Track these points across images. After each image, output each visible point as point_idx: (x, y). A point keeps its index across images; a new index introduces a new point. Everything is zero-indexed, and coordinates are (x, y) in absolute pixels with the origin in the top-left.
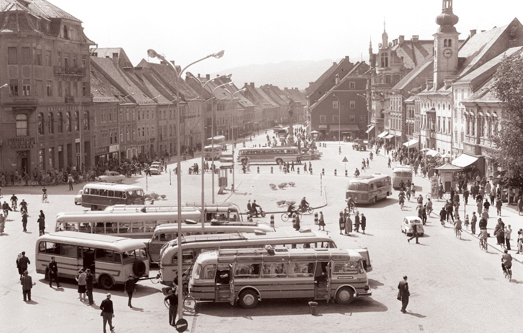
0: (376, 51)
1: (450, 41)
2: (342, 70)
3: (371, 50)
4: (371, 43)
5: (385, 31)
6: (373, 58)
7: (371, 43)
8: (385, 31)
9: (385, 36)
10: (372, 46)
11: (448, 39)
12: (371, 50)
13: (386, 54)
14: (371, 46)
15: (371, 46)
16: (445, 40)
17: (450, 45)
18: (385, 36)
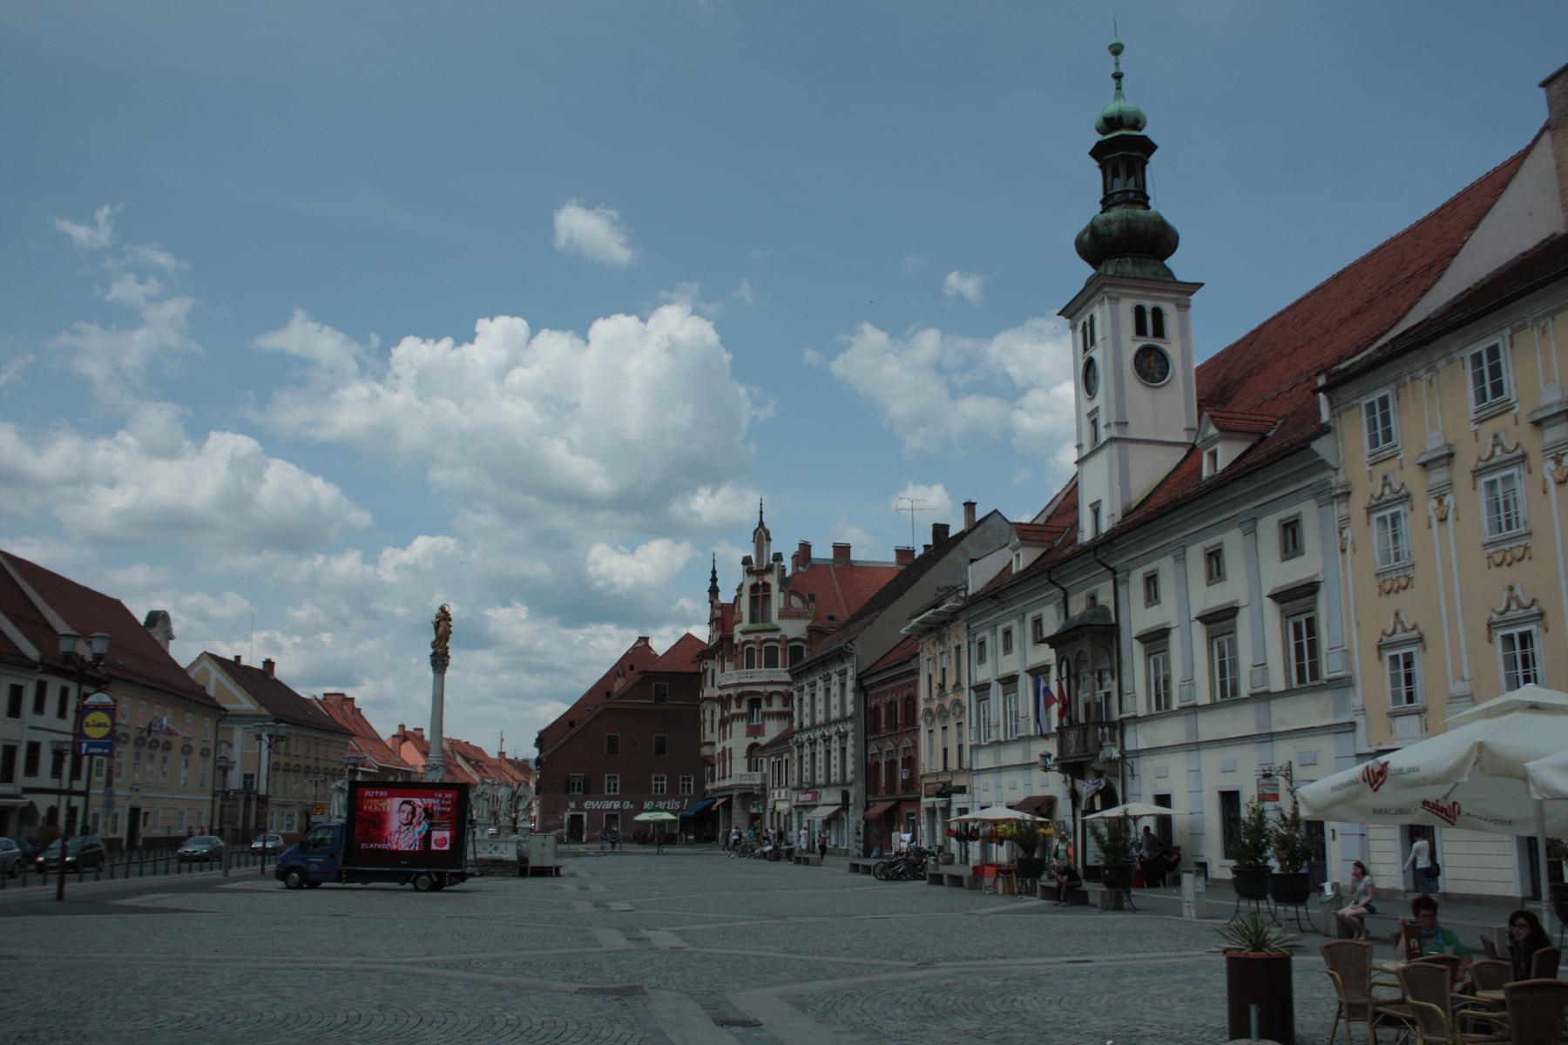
0: (726, 597)
1: (1158, 314)
2: (632, 668)
3: (714, 591)
4: (714, 572)
5: (761, 524)
6: (722, 617)
7: (714, 572)
8: (761, 524)
9: (762, 535)
10: (718, 584)
11: (1149, 305)
12: (714, 591)
13: (767, 586)
14: (714, 580)
15: (714, 580)
16: (1139, 312)
17: (1159, 332)
18: (762, 535)
